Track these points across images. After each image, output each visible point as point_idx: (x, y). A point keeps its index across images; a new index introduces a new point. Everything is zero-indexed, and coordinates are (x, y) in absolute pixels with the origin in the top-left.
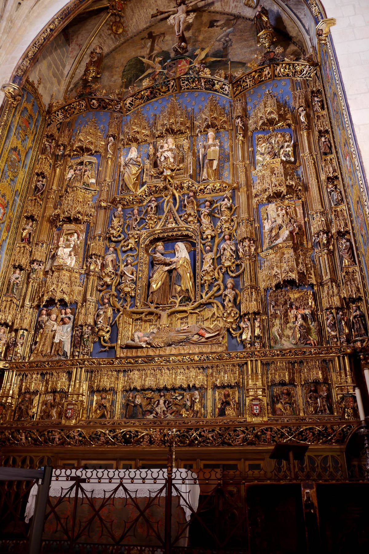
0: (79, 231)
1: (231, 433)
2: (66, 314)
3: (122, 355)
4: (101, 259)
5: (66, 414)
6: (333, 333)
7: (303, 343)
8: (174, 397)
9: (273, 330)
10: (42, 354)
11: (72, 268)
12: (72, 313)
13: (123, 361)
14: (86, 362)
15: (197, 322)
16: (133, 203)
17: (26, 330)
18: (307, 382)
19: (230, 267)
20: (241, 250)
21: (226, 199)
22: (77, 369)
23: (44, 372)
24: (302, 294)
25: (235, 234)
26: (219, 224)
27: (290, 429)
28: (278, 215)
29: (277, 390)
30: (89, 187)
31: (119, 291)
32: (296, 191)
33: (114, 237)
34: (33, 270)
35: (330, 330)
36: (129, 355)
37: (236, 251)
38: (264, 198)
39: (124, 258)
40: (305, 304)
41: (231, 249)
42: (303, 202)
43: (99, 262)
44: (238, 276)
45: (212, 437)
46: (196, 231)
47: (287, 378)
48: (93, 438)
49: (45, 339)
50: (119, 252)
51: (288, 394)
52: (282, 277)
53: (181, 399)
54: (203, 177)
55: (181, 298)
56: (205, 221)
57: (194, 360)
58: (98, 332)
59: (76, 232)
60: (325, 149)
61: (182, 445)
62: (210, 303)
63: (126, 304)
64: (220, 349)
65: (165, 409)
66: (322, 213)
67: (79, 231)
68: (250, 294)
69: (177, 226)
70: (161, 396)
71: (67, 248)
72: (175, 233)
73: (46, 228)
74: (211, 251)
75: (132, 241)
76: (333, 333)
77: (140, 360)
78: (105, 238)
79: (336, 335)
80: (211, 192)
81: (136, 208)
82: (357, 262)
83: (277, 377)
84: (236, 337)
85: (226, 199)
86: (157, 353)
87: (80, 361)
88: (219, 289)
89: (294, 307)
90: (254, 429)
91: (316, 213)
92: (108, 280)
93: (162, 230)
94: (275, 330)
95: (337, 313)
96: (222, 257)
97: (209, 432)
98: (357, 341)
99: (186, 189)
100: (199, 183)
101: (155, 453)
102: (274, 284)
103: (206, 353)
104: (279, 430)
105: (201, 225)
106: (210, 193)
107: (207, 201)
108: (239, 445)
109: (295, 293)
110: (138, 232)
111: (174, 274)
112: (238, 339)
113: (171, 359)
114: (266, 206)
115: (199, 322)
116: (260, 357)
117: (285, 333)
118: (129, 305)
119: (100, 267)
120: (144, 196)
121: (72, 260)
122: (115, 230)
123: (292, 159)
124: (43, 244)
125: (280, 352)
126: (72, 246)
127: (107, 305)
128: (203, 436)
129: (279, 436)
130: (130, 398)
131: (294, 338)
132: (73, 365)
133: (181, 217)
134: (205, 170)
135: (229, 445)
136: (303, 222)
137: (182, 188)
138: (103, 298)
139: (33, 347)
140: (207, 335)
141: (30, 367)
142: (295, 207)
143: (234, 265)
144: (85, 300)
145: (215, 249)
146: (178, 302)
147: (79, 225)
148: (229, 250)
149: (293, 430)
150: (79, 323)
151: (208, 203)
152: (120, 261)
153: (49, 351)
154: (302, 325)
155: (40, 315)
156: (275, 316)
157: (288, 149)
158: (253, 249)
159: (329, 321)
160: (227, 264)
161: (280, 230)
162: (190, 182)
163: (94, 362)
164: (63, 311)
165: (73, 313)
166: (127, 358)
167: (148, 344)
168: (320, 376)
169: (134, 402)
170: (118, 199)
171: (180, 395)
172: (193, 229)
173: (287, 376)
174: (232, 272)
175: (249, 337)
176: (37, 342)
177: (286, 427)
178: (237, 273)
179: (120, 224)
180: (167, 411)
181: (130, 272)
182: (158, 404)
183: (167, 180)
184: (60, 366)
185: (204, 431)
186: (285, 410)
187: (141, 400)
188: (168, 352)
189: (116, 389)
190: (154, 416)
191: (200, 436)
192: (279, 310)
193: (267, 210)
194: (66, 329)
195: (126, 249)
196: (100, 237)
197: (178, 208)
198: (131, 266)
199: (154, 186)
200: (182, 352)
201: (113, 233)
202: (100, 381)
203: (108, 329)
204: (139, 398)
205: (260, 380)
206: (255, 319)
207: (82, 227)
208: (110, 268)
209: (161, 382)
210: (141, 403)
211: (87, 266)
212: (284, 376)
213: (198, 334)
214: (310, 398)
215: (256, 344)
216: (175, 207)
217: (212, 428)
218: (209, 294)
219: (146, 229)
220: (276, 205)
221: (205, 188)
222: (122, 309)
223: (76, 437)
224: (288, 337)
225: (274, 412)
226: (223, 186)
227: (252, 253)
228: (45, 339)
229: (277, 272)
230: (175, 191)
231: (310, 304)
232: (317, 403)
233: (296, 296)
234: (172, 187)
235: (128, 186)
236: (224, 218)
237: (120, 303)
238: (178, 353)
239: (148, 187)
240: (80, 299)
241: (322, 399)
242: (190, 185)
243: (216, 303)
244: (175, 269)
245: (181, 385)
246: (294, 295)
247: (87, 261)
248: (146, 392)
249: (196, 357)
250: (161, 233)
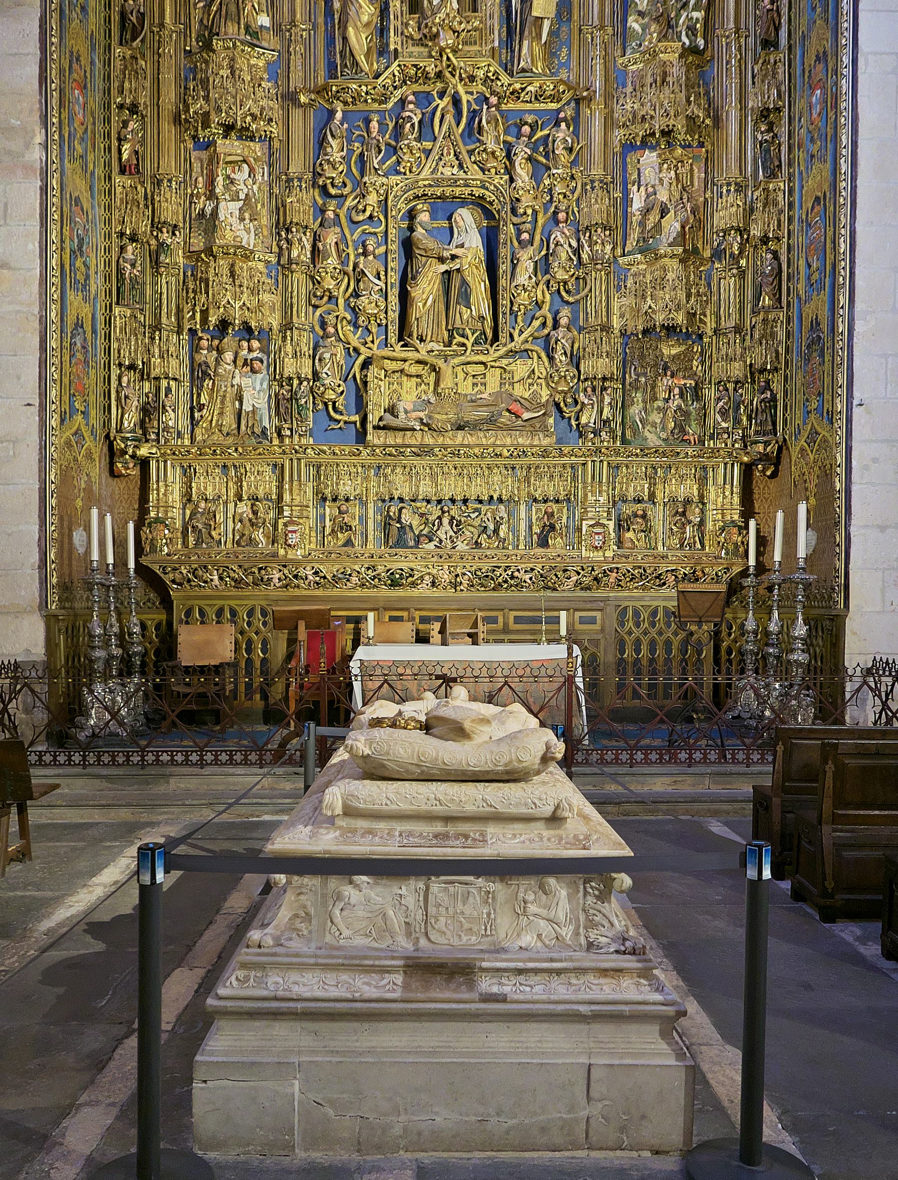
0: (252, 159)
1: (559, 574)
2: (250, 350)
3: (376, 441)
4: (308, 234)
5: (286, 540)
6: (724, 425)
7: (677, 439)
9: (631, 411)
10: (220, 431)
11: (252, 252)
12: (261, 350)
13: (377, 451)
14: (309, 451)
15: (501, 384)
16: (366, 101)
17: (176, 379)
18: (674, 500)
19: (565, 283)
20: (587, 248)
21: (563, 125)
22: (291, 459)
23: (229, 463)
24: (683, 348)
25: (576, 209)
26: (547, 182)
27: (645, 571)
28: (661, 180)
29: (627, 509)
30: (258, 39)
31: (354, 311)
32: (699, 126)
33: (333, 185)
34: (161, 245)
35: (720, 420)
36: (390, 441)
37: (577, 252)
38: (637, 135)
39: (356, 236)
40: (686, 368)
41: (570, 246)
42: (707, 151)
43: (306, 243)
44: (578, 301)
45: (531, 579)
46: (501, 192)
47: (646, 493)
48: (340, 579)
49: (222, 402)
50: (343, 220)
51: (644, 517)
52: (660, 318)
54: (522, 64)
55: (475, 335)
56: (523, 172)
57: (501, 455)
58: (323, 393)
59: (244, 161)
60: (766, 33)
61: (483, 589)
62: (526, 350)
63: (370, 338)
64: (546, 442)
66: (740, 188)
67: (252, 159)
68: (599, 340)
69: (462, 174)
70: (443, 512)
71: (233, 200)
72: (458, 191)
73: (170, 139)
74: (531, 242)
75: (372, 199)
76: (724, 425)
77: (409, 450)
78: (314, 184)
79: (728, 428)
80: (533, 99)
81: (375, 118)
82: (784, 304)
83: (631, 489)
84: (570, 418)
85: (563, 125)
86: (440, 440)
87: (297, 447)
88: (544, 324)
89: (669, 373)
90: (593, 570)
91: (729, 184)
92: (329, 284)
93: (433, 180)
94: (635, 410)
95: (735, 390)
96: (551, 258)
97: (526, 571)
98: (756, 442)
99: (479, 82)
100: (512, 76)
101: (438, 600)
102: (640, 328)
103: (523, 446)
104: (629, 571)
105: (512, 180)
106: (531, 102)
107: (526, 123)
108: (569, 590)
109: (673, 346)
110: (384, 180)
111: (456, 282)
112: (573, 423)
113: (462, 452)
114: (639, 153)
115: (505, 384)
116: (608, 456)
117: (650, 419)
118: (377, 342)
119: (308, 253)
120: (391, 88)
121: (248, 231)
122: (335, 168)
123: (701, 42)
124: (170, 181)
125: (641, 450)
126: (242, 196)
127: (333, 338)
128: (517, 578)
129: (628, 579)
130: (391, 514)
131: (664, 429)
132: (284, 452)
133: (471, 153)
134: (526, 43)
135: (555, 589)
136: (702, 199)
137: (472, 78)
138: (323, 324)
139: (196, 415)
140: (526, 416)
141: (200, 455)
142: (691, 165)
143: (574, 279)
144: (287, 326)
145: (537, 238)
146: (469, 345)
147: (252, 144)
148: (567, 246)
149: (648, 571)
150: (286, 375)
151: (526, 129)
152: (350, 243)
153: (234, 426)
154: (679, 408)
155: (195, 348)
156: (635, 386)
157: (696, 15)
158: (608, 248)
159: (721, 404)
160: (561, 275)
161: (662, 217)
162: (492, 69)
163: (324, 452)
164: (245, 344)
165: (265, 350)
166: (385, 446)
167: (422, 423)
168: (696, 493)
169: (399, 521)
170: (334, 88)
171: (476, 510)
172: (495, 186)
173: (646, 491)
174: (568, 292)
175: (592, 421)
176: (204, 405)
177: (640, 567)
178: (578, 297)
179: (344, 154)
180: (457, 538)
181: (375, 273)
182: (441, 524)
183: (445, 58)
184: (260, 454)
185: (518, 570)
186: (638, 540)
188: (459, 440)
189: (364, 499)
191: (512, 577)
192: (645, 375)
193: (639, 160)
194: (258, 383)
195: (361, 218)
196: (300, 180)
197: (464, 130)
198: (374, 257)
199: (413, 65)
200: (484, 441)
201: (333, 178)
202: (337, 484)
203: (341, 389)
205: (605, 494)
206: (604, 389)
207: (257, 148)
208: (332, 261)
209: (446, 490)
211: (280, 248)
212: (643, 490)
213: (509, 411)
214: (675, 525)
215: (603, 434)
216: (458, 125)
217: (531, 565)
218: (524, 336)
219: (398, 173)
220: (659, 156)
221: (523, 89)
222: (363, 349)
223: (311, 577)
224: (654, 425)
225: (620, 543)
226: (558, 91)
227: (607, 257)
228: (222, 402)
229: (650, 307)
230: (461, 90)
231: (695, 369)
232: (685, 532)
233: (674, 352)
234: (454, 76)
235: (358, 58)
236: (560, 171)
237: (357, 336)
238: (477, 442)
239: (399, 66)
240: (275, 321)
241: (693, 526)
242: (490, 74)
243: (537, 352)
244: (458, 270)
246: (670, 350)
247: (279, 234)
248: (419, 504)
249: (505, 451)
250: (430, 186)
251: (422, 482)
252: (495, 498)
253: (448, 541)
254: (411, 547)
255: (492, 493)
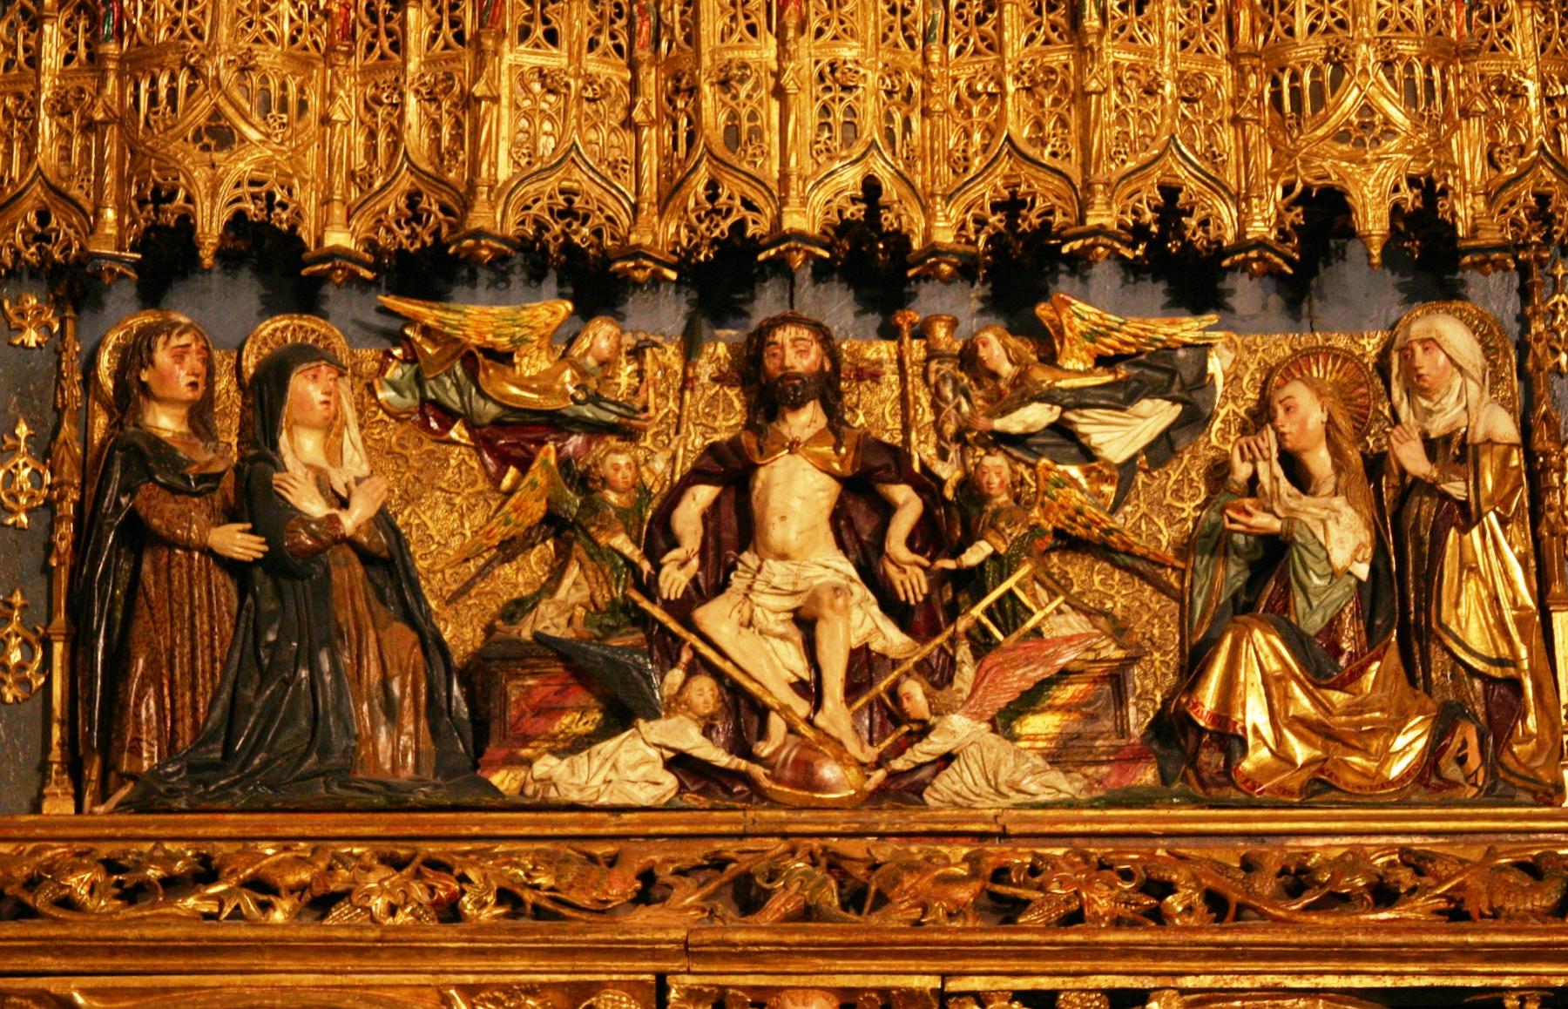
8: (1036, 416)
53: (1162, 449)
65: (892, 639)
180: (939, 674)
187: (375, 451)
190: (680, 763)
204: (331, 427)
210: (383, 519)
245: (1171, 202)
251: (516, 57)
252: (1373, 220)
253: (836, 715)
254: (396, 801)
255: (1332, 166)
